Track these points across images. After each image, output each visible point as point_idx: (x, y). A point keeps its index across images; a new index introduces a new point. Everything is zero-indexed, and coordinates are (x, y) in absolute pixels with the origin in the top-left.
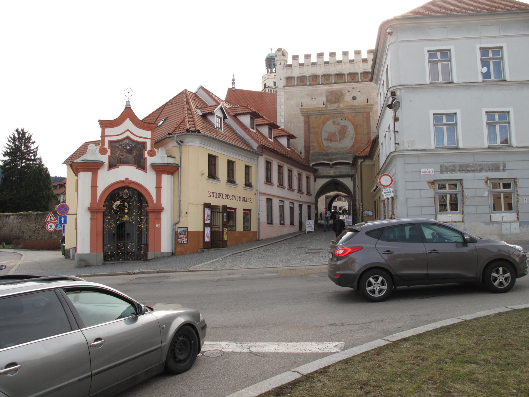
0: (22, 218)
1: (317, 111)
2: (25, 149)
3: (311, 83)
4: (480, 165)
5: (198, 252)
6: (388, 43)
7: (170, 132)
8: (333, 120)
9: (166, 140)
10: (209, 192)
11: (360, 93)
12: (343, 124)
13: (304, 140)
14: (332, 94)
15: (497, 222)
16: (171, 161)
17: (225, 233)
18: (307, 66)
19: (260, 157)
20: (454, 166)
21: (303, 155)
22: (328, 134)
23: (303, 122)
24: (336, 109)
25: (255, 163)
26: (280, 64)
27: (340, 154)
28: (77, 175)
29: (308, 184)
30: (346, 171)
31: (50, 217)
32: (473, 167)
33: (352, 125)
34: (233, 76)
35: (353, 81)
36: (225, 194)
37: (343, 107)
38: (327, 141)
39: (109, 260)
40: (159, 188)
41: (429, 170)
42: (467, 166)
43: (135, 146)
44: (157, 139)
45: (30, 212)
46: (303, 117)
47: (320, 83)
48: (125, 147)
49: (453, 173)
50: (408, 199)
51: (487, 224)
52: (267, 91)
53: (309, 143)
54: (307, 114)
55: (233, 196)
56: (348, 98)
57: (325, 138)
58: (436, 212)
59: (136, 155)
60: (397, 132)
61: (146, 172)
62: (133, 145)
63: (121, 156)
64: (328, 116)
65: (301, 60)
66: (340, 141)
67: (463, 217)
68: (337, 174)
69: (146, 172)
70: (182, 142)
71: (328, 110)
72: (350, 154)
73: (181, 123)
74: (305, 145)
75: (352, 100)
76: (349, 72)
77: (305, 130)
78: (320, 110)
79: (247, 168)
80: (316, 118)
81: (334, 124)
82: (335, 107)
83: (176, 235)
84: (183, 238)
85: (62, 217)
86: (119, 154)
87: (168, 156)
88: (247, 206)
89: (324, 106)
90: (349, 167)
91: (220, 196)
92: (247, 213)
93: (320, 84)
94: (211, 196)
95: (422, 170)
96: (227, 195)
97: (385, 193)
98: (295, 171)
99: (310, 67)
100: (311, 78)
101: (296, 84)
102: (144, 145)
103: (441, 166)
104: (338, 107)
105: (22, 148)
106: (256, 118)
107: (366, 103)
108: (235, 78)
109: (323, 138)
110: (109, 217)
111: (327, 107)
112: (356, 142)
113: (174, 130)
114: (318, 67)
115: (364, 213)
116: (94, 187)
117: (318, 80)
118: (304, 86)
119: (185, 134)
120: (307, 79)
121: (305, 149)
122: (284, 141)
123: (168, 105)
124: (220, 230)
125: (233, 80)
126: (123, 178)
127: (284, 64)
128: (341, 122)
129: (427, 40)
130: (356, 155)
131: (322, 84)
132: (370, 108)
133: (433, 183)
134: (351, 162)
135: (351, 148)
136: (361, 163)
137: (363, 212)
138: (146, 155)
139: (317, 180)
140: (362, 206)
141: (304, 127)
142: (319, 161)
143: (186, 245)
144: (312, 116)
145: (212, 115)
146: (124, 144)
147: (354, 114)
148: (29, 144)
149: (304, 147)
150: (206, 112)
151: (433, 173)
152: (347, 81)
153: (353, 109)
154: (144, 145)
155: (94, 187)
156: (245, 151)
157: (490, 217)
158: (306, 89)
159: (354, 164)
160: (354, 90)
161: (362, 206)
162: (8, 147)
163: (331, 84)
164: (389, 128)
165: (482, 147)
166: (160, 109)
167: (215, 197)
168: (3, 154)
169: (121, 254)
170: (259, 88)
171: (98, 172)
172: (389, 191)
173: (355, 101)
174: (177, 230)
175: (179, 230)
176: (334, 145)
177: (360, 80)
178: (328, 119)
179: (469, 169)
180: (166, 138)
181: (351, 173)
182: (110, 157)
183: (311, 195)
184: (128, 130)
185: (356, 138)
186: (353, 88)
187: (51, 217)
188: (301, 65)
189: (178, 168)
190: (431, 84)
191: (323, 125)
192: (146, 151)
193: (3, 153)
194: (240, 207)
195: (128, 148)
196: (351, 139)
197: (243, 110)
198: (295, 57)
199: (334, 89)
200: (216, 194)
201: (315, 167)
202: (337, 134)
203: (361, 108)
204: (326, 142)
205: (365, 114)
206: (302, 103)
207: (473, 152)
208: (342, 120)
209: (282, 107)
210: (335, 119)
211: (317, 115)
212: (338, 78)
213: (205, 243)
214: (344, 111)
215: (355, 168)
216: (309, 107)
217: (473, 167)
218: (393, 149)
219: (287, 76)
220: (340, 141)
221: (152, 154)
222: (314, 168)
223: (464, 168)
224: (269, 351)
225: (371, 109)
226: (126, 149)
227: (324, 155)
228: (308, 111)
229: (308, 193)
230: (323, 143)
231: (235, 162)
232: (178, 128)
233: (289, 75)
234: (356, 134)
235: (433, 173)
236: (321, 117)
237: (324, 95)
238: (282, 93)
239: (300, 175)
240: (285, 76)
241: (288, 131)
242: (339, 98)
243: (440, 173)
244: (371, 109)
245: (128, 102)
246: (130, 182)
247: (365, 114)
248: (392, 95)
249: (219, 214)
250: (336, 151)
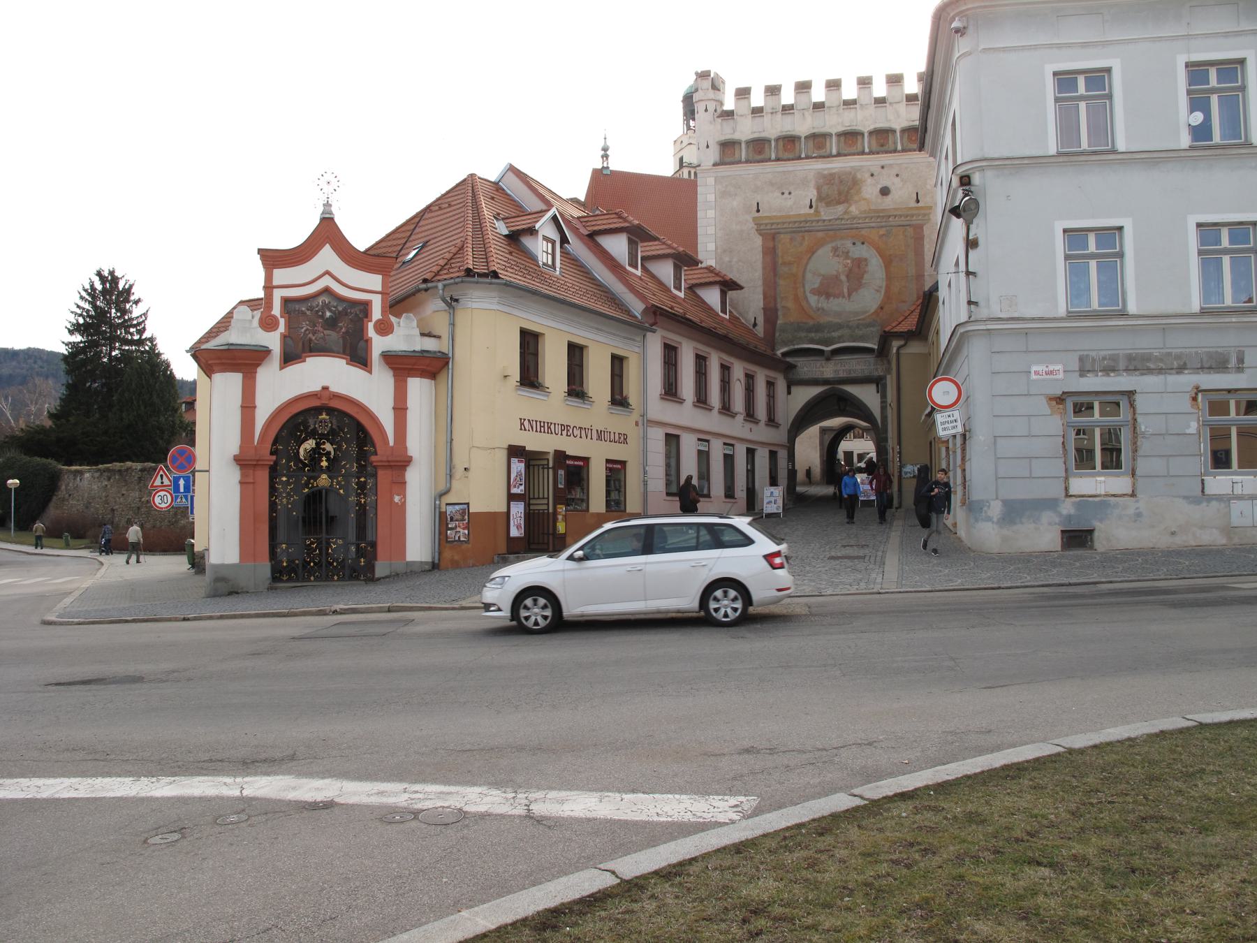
0: (109, 479)
1: (795, 222)
2: (119, 318)
3: (781, 155)
4: (1178, 357)
5: (493, 562)
6: (957, 55)
7: (428, 276)
8: (834, 244)
9: (419, 295)
10: (521, 419)
11: (898, 179)
12: (856, 256)
15: (1219, 498)
16: (430, 345)
17: (560, 517)
18: (772, 113)
19: (649, 335)
20: (1114, 358)
21: (760, 331)
23: (760, 249)
24: (842, 219)
25: (637, 350)
26: (706, 110)
27: (849, 327)
28: (210, 378)
29: (771, 399)
30: (863, 367)
31: (159, 477)
32: (1161, 360)
34: (605, 138)
35: (883, 149)
36: (562, 425)
37: (857, 212)
39: (285, 578)
40: (400, 409)
41: (1051, 368)
42: (1147, 358)
43: (345, 309)
44: (397, 292)
45: (129, 464)
46: (761, 238)
47: (803, 156)
48: (320, 313)
49: (1112, 374)
50: (998, 439)
51: (1194, 500)
52: (686, 176)
53: (775, 300)
55: (581, 428)
56: (870, 191)
58: (1066, 470)
59: (347, 332)
60: (974, 274)
61: (370, 372)
62: (340, 309)
63: (310, 335)
64: (820, 234)
65: (757, 99)
66: (850, 295)
67: (1134, 484)
68: (842, 375)
69: (370, 372)
70: (457, 300)
72: (873, 326)
73: (455, 255)
76: (872, 127)
77: (764, 268)
79: (618, 362)
80: (791, 239)
81: (837, 253)
82: (839, 214)
83: (442, 521)
84: (458, 529)
85: (179, 478)
86: (307, 330)
87: (422, 335)
88: (617, 452)
89: (812, 211)
90: (870, 358)
91: (549, 428)
92: (616, 471)
93: (803, 159)
94: (525, 430)
95: (1034, 368)
96: (567, 426)
97: (942, 423)
98: (739, 370)
99: (779, 116)
100: (781, 143)
101: (743, 159)
102: (365, 307)
103: (1081, 359)
104: (846, 213)
105: (111, 314)
106: (642, 241)
107: (913, 204)
108: (608, 144)
109: (808, 288)
110: (284, 479)
112: (888, 296)
113: (438, 272)
114: (797, 115)
115: (904, 470)
116: (248, 408)
117: (797, 148)
118: (763, 162)
119: (462, 282)
120: (770, 145)
121: (765, 314)
122: (712, 297)
123: (431, 211)
124: (548, 509)
125: (605, 149)
126: (317, 388)
127: (715, 111)
128: (852, 248)
129: (1051, 46)
130: (887, 329)
131: (807, 157)
132: (925, 215)
133: (1060, 399)
135: (876, 313)
136: (898, 349)
137: (901, 467)
138: (371, 332)
139: (794, 389)
140: (900, 453)
141: (764, 263)
142: (798, 344)
143: (466, 545)
144: (782, 236)
145: (531, 234)
146: (318, 306)
147: (884, 229)
148: (128, 306)
149: (762, 311)
150: (518, 228)
151: (1061, 376)
152: (867, 150)
153: (883, 217)
154: (365, 307)
155: (248, 408)
156: (611, 321)
157: (1203, 484)
158: (768, 170)
159: (882, 352)
160: (884, 171)
161: (900, 453)
162: (79, 311)
163: (828, 157)
164: (957, 264)
165: (1186, 310)
166: (412, 222)
167: (536, 431)
168: (69, 329)
169: (312, 564)
170: (665, 167)
171: (256, 372)
172: (952, 419)
173: (888, 199)
174: (443, 509)
175: (450, 509)
176: (834, 305)
177: (899, 148)
178: (820, 244)
179: (1152, 366)
180: (419, 291)
181: (876, 374)
182: (284, 337)
183: (777, 426)
184: (328, 273)
185: (888, 288)
186: (883, 167)
187: (162, 476)
188: (757, 111)
189: (447, 363)
190: (1059, 154)
191: (810, 258)
192: (371, 321)
193: (69, 327)
194: (598, 455)
195: (328, 314)
196: (878, 291)
197: (611, 221)
198: (743, 93)
199: (836, 170)
200: (538, 423)
201: (789, 359)
202: (843, 278)
203: (901, 216)
204: (816, 297)
207: (1162, 323)
208: (854, 244)
209: (711, 213)
210: (839, 243)
211: (794, 232)
212: (845, 142)
213: (511, 540)
215: (885, 362)
216: (774, 214)
217: (1161, 360)
218: (964, 318)
219: (723, 138)
220: (850, 295)
221: (384, 328)
222: (788, 362)
223: (1139, 364)
224: (572, 814)
225: (926, 218)
226: (322, 317)
227: (809, 330)
228: (772, 224)
229: (772, 421)
230: (807, 301)
231: (586, 347)
232: (447, 267)
233: (728, 136)
234: (889, 277)
235: (1061, 376)
236: (803, 237)
237: (812, 184)
238: (711, 181)
239: (750, 377)
240: (717, 140)
241: (724, 272)
242: (847, 192)
243: (1077, 374)
245: (327, 205)
246: (334, 396)
247: (910, 231)
248: (962, 184)
249: (546, 470)
250: (839, 321)
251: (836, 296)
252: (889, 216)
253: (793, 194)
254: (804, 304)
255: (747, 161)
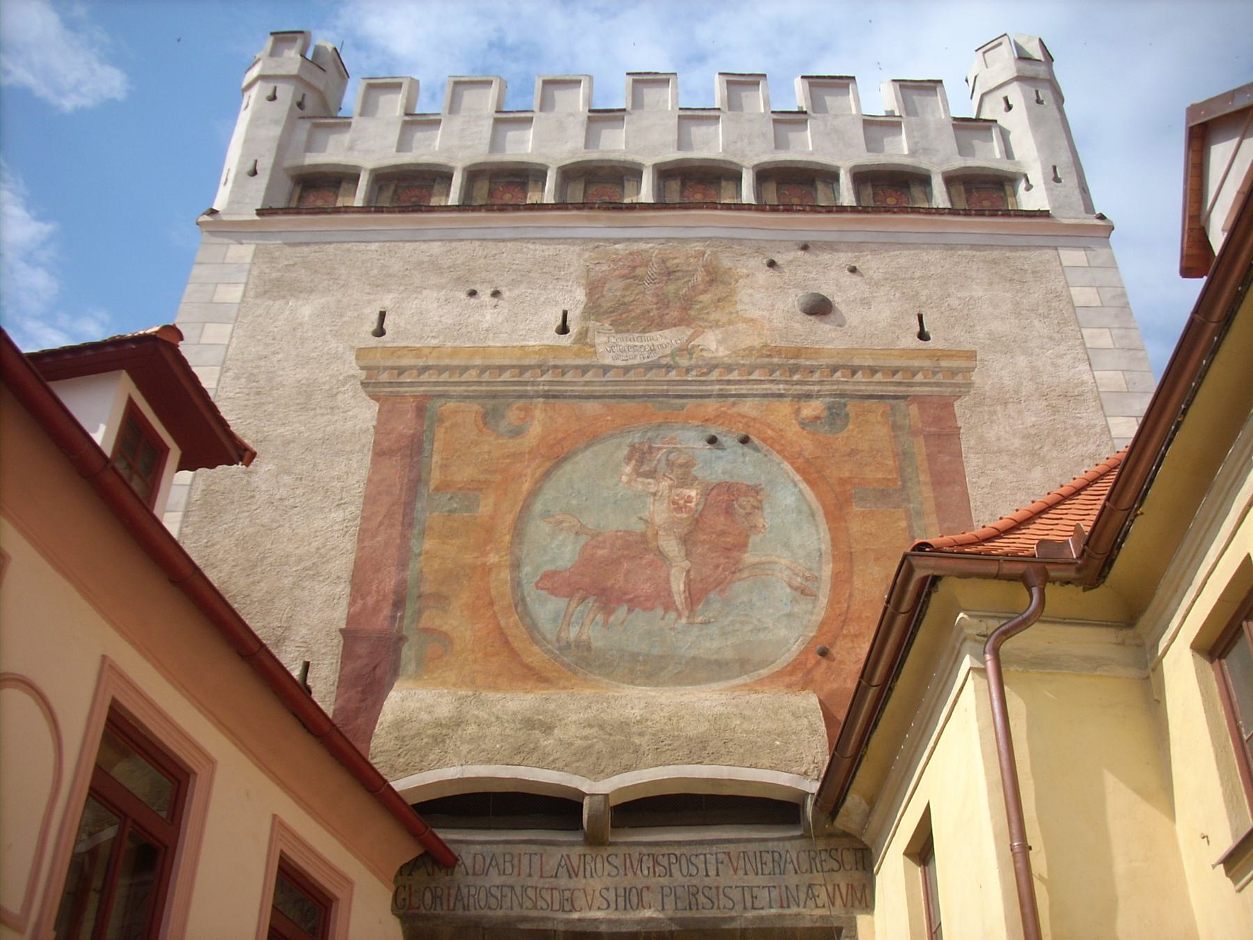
8: (636, 438)
11: (855, 278)
13: (346, 575)
14: (634, 268)
22: (583, 539)
23: (369, 439)
24: (669, 368)
33: (803, 486)
37: (722, 353)
38: (570, 596)
54: (412, 384)
57: (555, 573)
64: (591, 407)
71: (593, 366)
74: (351, 618)
75: (801, 316)
77: (370, 499)
78: (526, 362)
80: (485, 416)
81: (646, 468)
89: (565, 340)
100: (482, 188)
111: (593, 346)
121: (348, 654)
132: (953, 372)
134: (813, 787)
144: (452, 405)
149: (338, 640)
191: (547, 474)
196: (803, 591)
202: (671, 546)
203: (873, 371)
205: (914, 410)
206: (382, 315)
208: (712, 441)
211: (494, 396)
214: (729, 382)
216: (434, 342)
225: (959, 379)
240: (288, 163)
244: (959, 379)
251: (633, 604)
252: (834, 369)
253: (506, 294)
254: (510, 622)
255: (364, 210)
